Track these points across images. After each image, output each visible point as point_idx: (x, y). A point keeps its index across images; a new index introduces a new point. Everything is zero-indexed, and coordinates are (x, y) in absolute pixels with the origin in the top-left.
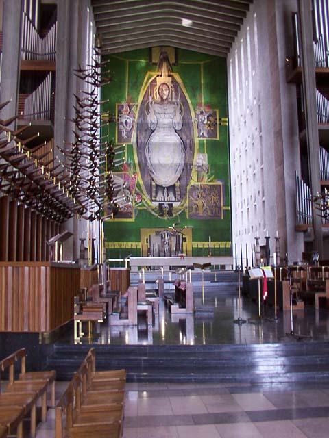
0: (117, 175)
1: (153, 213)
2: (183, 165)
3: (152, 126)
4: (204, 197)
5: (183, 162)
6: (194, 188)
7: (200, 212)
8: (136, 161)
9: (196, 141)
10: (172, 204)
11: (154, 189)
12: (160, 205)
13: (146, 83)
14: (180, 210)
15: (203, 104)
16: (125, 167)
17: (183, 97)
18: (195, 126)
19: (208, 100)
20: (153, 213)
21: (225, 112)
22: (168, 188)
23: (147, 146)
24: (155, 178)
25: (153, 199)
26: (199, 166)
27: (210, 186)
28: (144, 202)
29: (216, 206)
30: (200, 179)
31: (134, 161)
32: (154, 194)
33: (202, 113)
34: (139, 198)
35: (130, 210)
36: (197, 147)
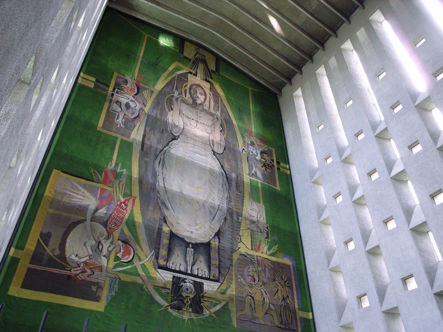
0: (84, 186)
1: (158, 298)
2: (226, 211)
3: (174, 130)
4: (264, 284)
5: (225, 206)
8: (135, 174)
9: (247, 179)
10: (202, 284)
11: (165, 241)
12: (177, 282)
13: (172, 73)
14: (220, 301)
15: (254, 134)
16: (106, 175)
18: (244, 158)
20: (158, 298)
22: (196, 246)
23: (161, 156)
24: (170, 219)
25: (162, 262)
26: (253, 222)
27: (274, 263)
28: (138, 264)
29: (286, 307)
30: (255, 246)
31: (130, 170)
32: (163, 252)
33: (252, 144)
34: (127, 252)
35: (97, 277)
36: (247, 190)
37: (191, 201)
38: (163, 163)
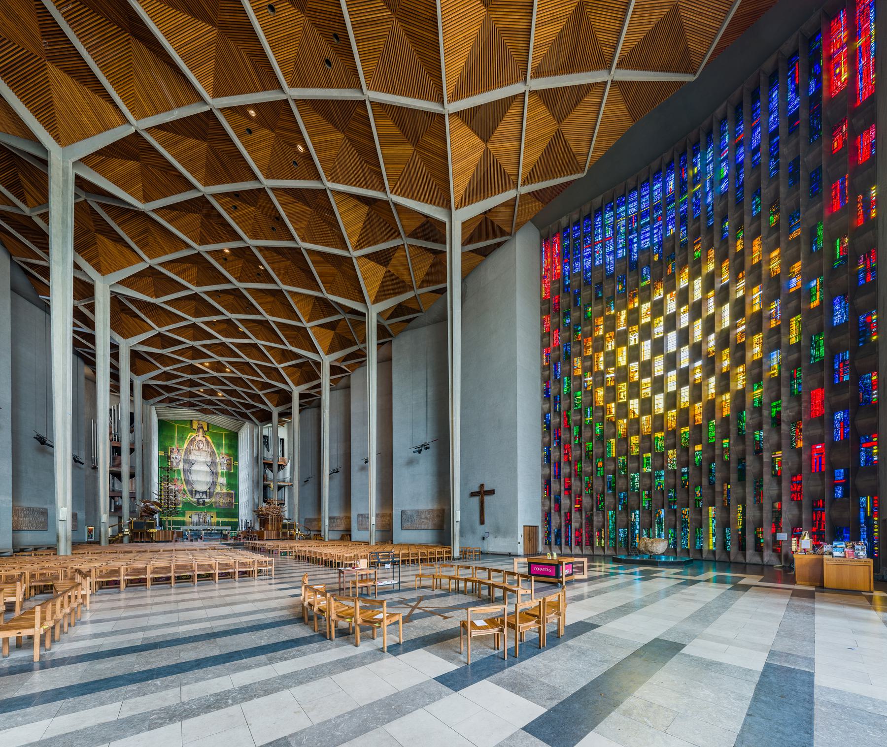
6: (218, 494)
7: (221, 505)
8: (183, 478)
9: (220, 471)
12: (198, 501)
17: (212, 448)
19: (227, 452)
21: (236, 458)
36: (220, 474)
37: (200, 482)
38: (190, 473)
